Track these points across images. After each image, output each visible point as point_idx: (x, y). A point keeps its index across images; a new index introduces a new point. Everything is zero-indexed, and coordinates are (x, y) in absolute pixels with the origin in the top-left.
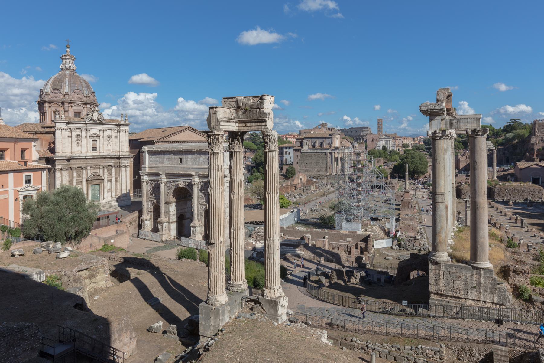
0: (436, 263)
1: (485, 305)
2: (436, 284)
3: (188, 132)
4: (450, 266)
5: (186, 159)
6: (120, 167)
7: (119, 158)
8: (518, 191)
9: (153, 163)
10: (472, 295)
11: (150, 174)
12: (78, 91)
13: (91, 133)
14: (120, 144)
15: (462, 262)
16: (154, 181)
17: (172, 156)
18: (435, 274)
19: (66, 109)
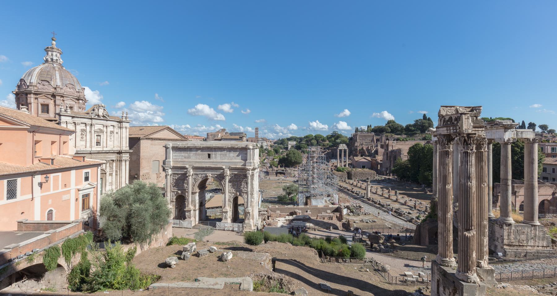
0: (510, 225)
1: (538, 249)
2: (509, 239)
3: (166, 131)
4: (518, 226)
5: (215, 155)
6: (121, 161)
7: (120, 153)
8: (364, 174)
9: (177, 157)
10: (531, 243)
11: (174, 168)
12: (71, 86)
13: (96, 128)
14: (117, 140)
15: (520, 223)
16: (177, 174)
17: (199, 152)
18: (508, 232)
19: (58, 102)
